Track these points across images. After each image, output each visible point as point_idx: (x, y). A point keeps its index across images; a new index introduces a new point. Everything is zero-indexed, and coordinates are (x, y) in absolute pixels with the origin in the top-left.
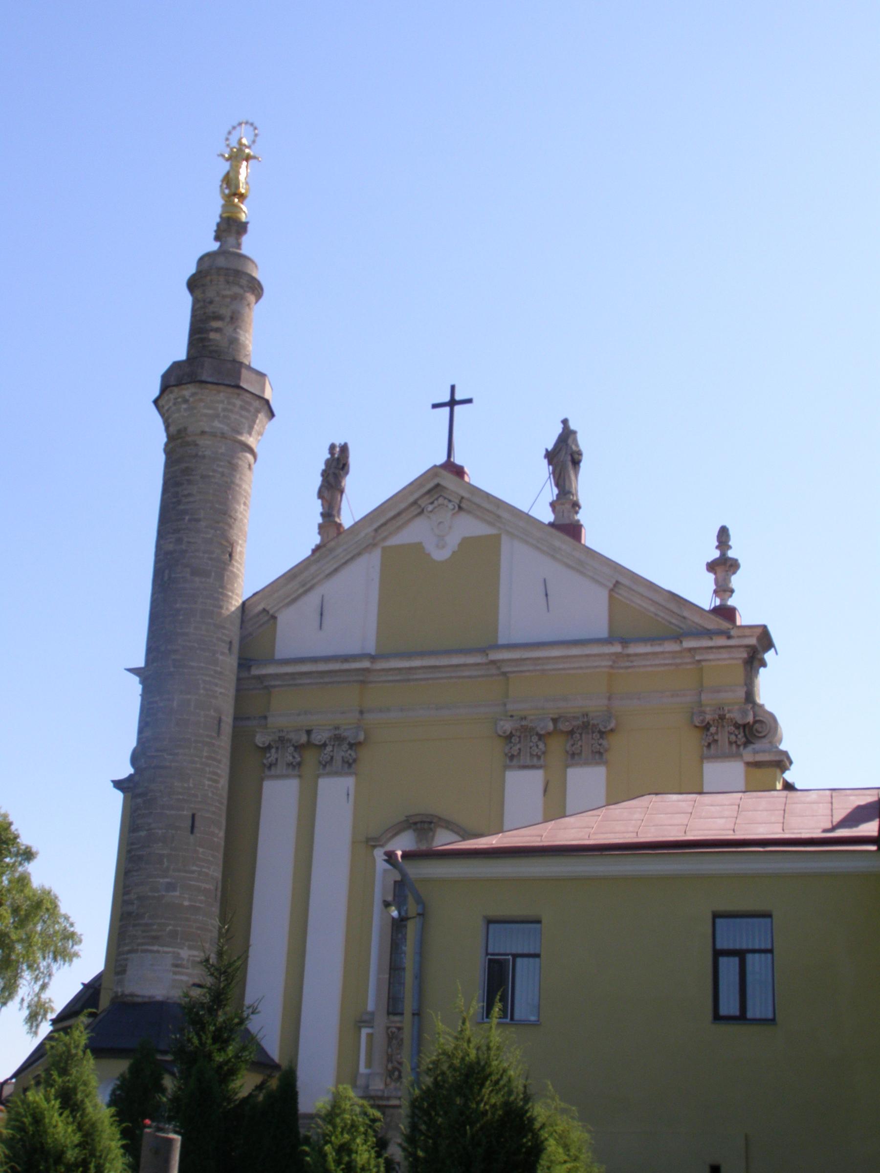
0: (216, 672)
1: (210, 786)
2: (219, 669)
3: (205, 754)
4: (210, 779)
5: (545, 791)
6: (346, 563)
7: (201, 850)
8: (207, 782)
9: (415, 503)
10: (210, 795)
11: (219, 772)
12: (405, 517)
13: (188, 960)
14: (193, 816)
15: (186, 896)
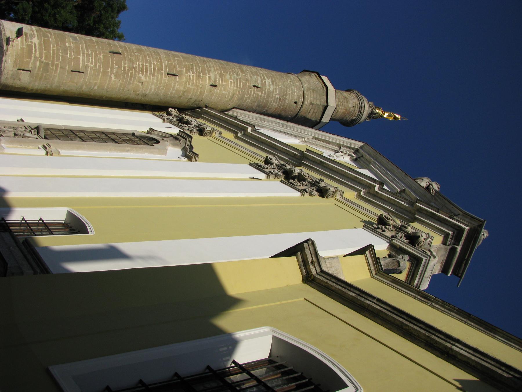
0: (199, 73)
1: (139, 65)
2: (201, 75)
3: (156, 63)
4: (143, 65)
5: (253, 178)
6: (286, 133)
7: (102, 56)
8: (141, 63)
9: (340, 146)
10: (135, 66)
11: (148, 74)
12: (330, 146)
13: (32, 42)
14: (120, 54)
15: (72, 45)
